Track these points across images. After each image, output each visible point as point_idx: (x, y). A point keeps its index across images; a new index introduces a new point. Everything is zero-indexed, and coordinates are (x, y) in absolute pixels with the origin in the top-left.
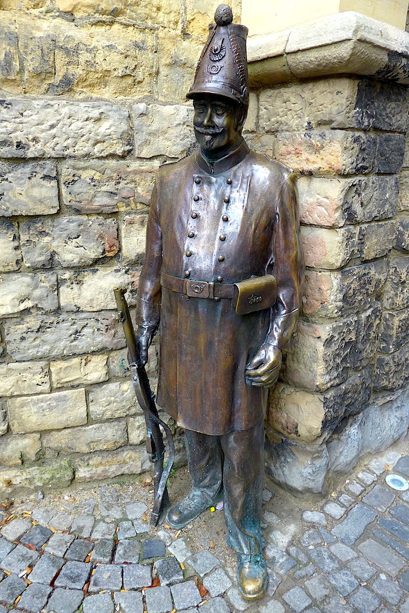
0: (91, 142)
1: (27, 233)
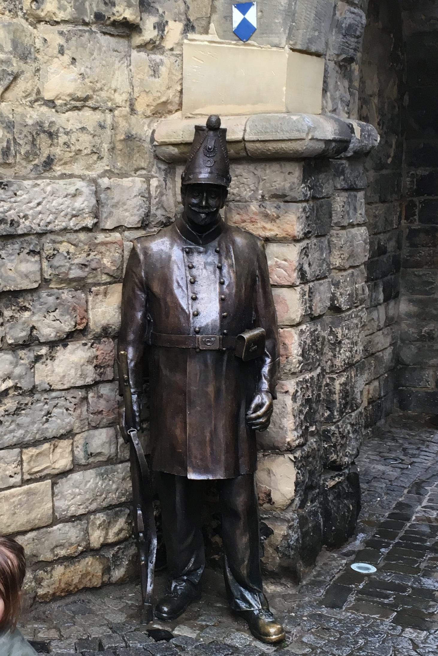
0: (69, 217)
1: (9, 309)
